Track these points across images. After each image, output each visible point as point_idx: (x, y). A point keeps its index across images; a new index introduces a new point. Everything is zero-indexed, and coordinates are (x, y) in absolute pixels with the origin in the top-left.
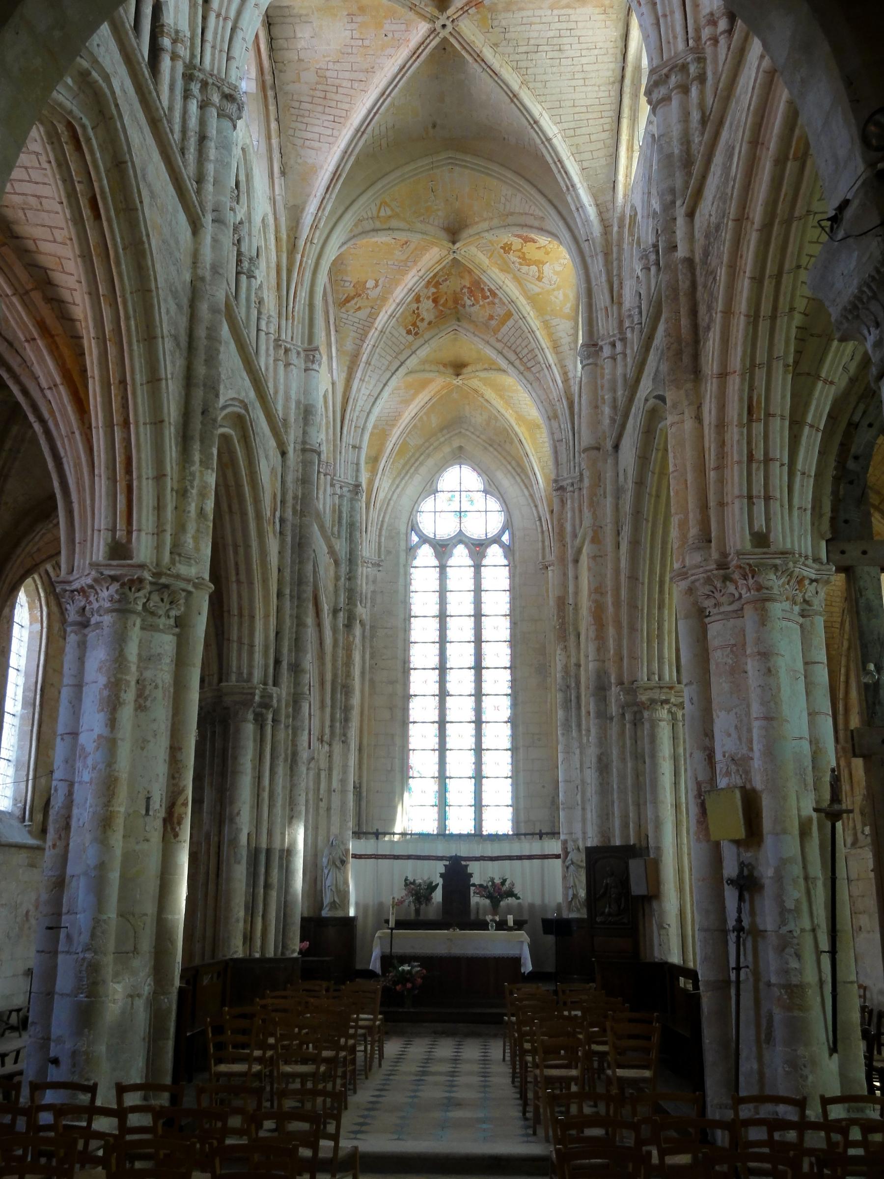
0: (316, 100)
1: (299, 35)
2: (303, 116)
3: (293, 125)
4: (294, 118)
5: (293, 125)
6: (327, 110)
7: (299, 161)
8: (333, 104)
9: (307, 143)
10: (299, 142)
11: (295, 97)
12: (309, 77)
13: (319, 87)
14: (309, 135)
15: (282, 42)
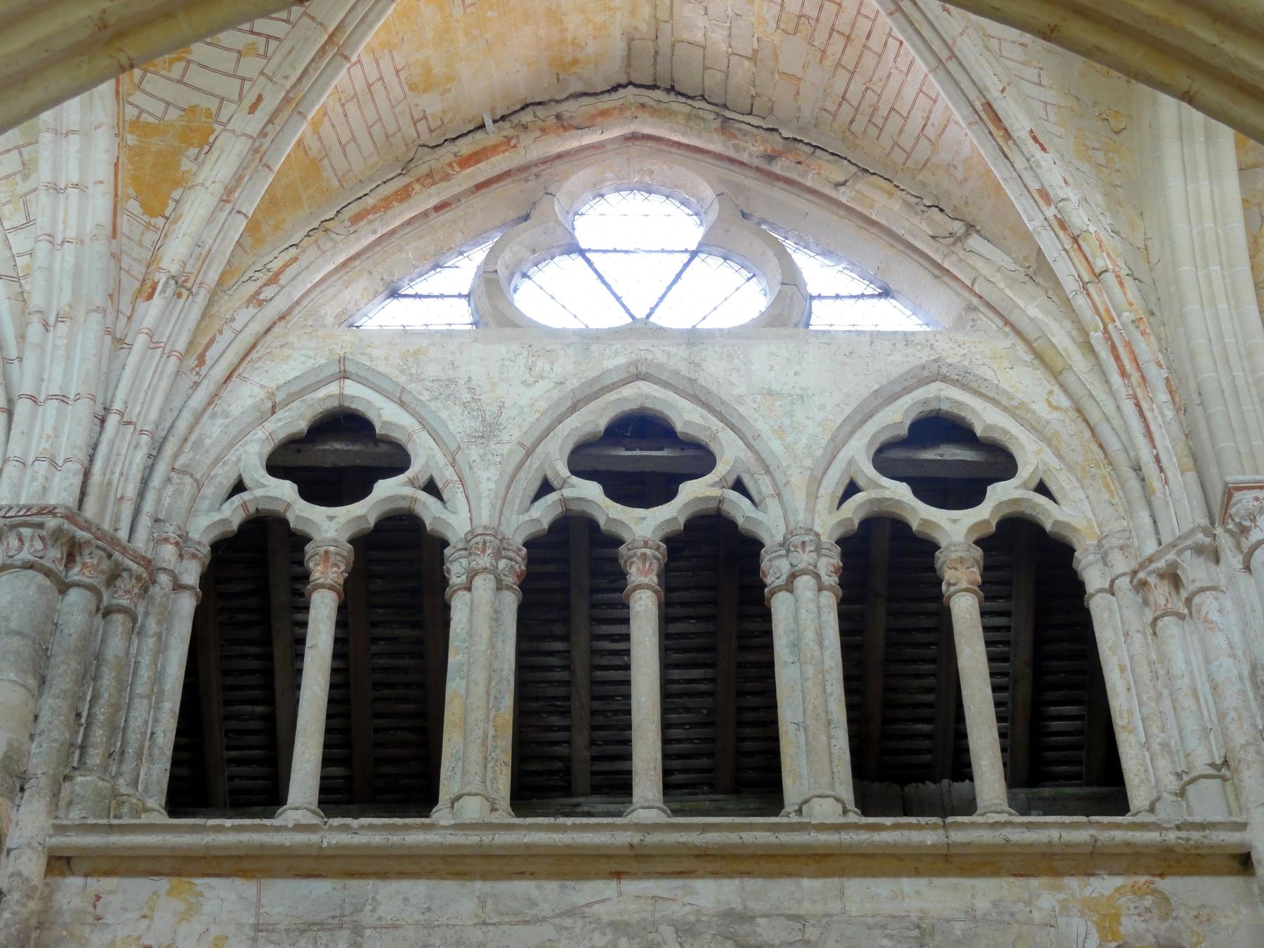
0: (850, 59)
1: (699, 37)
2: (875, 108)
3: (886, 141)
4: (873, 132)
5: (886, 141)
6: (875, 44)
7: (959, 174)
8: (864, 25)
9: (930, 131)
10: (923, 150)
11: (831, 107)
12: (793, 55)
13: (819, 41)
14: (917, 118)
15: (712, 81)
